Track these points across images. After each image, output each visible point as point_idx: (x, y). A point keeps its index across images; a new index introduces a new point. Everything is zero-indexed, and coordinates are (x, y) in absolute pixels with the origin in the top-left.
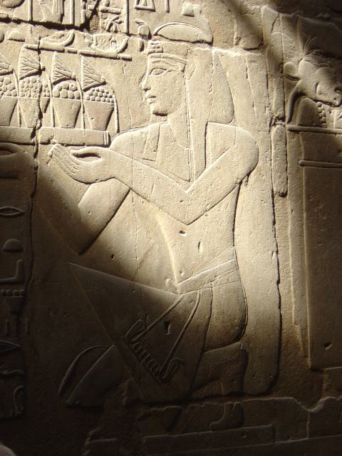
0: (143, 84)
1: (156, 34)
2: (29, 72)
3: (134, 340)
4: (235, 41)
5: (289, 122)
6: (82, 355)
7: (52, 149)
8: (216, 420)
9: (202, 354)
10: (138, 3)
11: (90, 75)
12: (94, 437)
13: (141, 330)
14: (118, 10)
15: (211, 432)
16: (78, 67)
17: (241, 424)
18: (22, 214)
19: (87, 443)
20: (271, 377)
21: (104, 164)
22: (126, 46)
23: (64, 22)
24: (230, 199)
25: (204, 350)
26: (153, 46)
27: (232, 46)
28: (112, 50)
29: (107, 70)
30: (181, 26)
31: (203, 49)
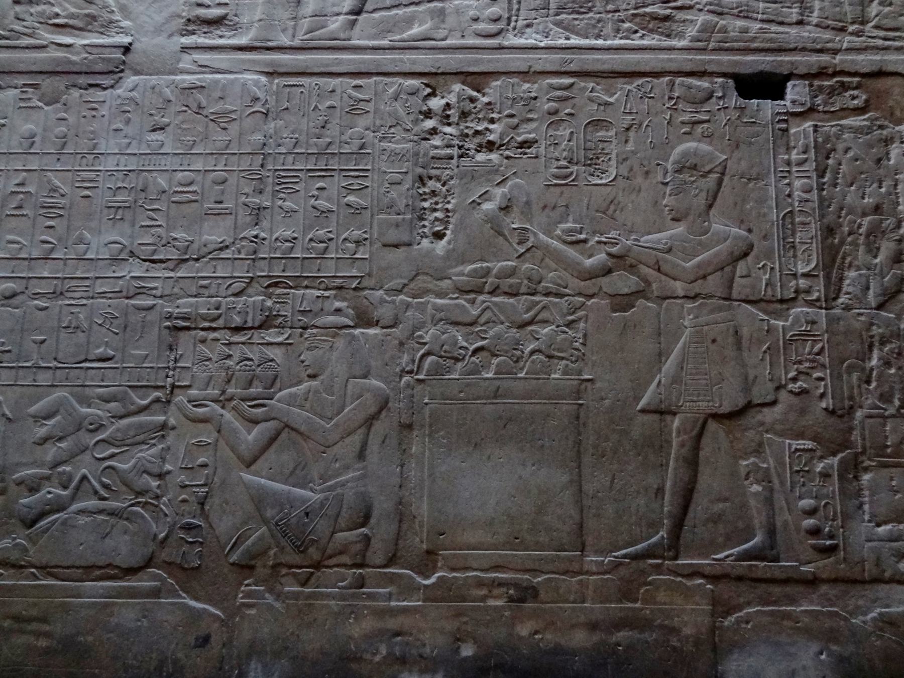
0: (302, 357)
5: (417, 374)
12: (247, 585)
16: (253, 353)
17: (362, 587)
19: (243, 588)
22: (290, 336)
25: (333, 533)
28: (280, 339)
29: (276, 354)
30: (331, 319)
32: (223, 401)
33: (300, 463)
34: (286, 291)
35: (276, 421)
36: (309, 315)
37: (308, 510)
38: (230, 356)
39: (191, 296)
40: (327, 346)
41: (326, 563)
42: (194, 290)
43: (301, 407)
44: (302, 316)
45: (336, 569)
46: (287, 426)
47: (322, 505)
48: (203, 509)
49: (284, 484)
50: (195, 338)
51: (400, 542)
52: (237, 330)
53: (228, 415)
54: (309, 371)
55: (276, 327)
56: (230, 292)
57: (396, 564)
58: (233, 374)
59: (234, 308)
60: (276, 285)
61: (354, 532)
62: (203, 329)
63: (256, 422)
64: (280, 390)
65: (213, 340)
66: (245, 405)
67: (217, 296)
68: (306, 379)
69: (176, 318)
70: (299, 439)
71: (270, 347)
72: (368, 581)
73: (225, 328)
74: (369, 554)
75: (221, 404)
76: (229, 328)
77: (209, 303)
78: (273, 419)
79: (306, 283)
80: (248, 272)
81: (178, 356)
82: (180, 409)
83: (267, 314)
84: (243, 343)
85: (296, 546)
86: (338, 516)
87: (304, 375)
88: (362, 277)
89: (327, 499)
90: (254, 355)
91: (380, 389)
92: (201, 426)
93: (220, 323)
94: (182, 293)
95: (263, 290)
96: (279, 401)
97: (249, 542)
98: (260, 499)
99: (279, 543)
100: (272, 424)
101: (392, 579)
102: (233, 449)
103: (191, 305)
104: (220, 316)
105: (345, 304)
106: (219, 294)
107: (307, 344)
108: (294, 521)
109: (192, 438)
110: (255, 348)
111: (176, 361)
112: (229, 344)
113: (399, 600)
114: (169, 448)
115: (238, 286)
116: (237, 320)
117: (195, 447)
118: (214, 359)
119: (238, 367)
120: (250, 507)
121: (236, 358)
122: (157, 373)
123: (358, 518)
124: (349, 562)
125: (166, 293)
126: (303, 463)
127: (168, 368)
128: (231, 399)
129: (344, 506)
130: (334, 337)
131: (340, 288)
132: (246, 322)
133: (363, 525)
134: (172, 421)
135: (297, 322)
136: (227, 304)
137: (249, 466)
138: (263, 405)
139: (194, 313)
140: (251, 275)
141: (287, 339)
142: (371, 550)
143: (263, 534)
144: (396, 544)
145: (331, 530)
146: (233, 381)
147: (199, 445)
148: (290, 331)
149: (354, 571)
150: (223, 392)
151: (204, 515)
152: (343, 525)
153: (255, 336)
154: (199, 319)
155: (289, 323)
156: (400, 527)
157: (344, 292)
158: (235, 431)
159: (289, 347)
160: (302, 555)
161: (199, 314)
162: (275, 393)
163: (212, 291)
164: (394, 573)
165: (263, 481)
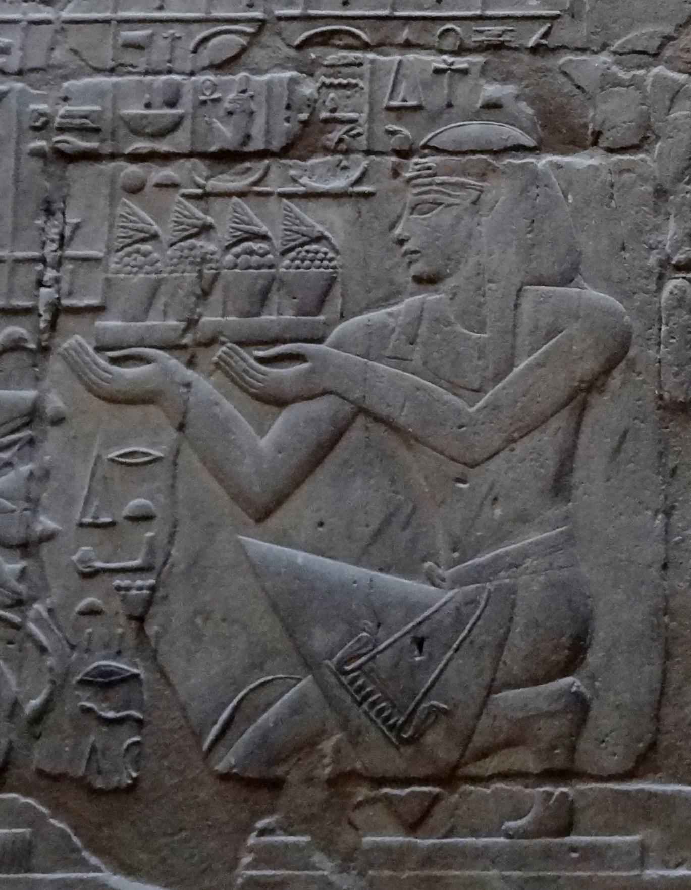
0: (397, 231)
1: (425, 147)
2: (186, 233)
3: (348, 668)
4: (590, 139)
6: (252, 690)
7: (219, 353)
8: (516, 819)
9: (488, 696)
10: (391, 98)
11: (295, 228)
13: (364, 650)
14: (353, 115)
15: (502, 839)
16: (270, 220)
17: (568, 829)
18: (157, 460)
20: (641, 745)
21: (312, 371)
23: (246, 149)
24: (561, 422)
25: (491, 689)
26: (418, 167)
27: (585, 148)
28: (339, 183)
30: (474, 128)
31: (518, 162)
32: (190, 347)
33: (398, 508)
34: (352, 55)
35: (331, 398)
36: (419, 117)
37: (424, 629)
38: (206, 229)
39: (98, 70)
40: (464, 198)
41: (472, 770)
42: (107, 57)
43: (399, 360)
44: (399, 120)
45: (499, 785)
46: (361, 410)
47: (459, 619)
48: (141, 630)
49: (357, 563)
50: (113, 181)
51: (665, 711)
52: (226, 158)
53: (205, 384)
54: (418, 268)
55: (327, 150)
56: (205, 57)
57: (656, 770)
58: (215, 277)
59: (216, 101)
60: (324, 39)
61: (541, 688)
62: (135, 158)
63: (281, 403)
64: (343, 317)
65: (159, 185)
66: (249, 357)
67: (170, 72)
68: (412, 286)
69: (61, 130)
70: (392, 442)
71: (312, 204)
72: (583, 819)
73: (190, 155)
74: (584, 745)
75: (186, 356)
76: (203, 156)
77: (150, 87)
78: (325, 393)
79: (405, 34)
80: (250, 6)
81: (67, 233)
82: (77, 370)
83: (304, 116)
84: (242, 194)
85: (391, 728)
86: (501, 647)
87: (404, 277)
88: (557, 17)
89: (472, 602)
90: (271, 224)
91: (608, 312)
92: (135, 413)
93: (180, 141)
94: (74, 63)
95: (292, 53)
96: (337, 346)
97: (267, 718)
98: (293, 605)
99: (347, 720)
100: (321, 407)
101: (646, 809)
102: (220, 473)
103: (99, 94)
104: (176, 125)
105: (510, 89)
106: (176, 66)
107: (411, 195)
108: (385, 661)
109: (108, 446)
110: (272, 204)
111: (62, 242)
112: (205, 197)
113: (666, 865)
114: (47, 474)
115: (226, 44)
116: (225, 135)
117: (117, 471)
118: (165, 237)
119: (229, 258)
120: (267, 627)
121: (223, 234)
122: (12, 273)
123: (556, 649)
124: (533, 765)
125: (31, 64)
126: (408, 510)
127: (43, 260)
128: (210, 343)
129: (520, 620)
130: (482, 176)
131: (497, 47)
132: (248, 137)
133: (569, 667)
134: (55, 403)
135: (385, 138)
136: (198, 90)
137: (263, 515)
138: (298, 358)
139: (109, 115)
140: (258, 14)
141: (359, 181)
142: (590, 733)
143: (303, 695)
144: (657, 718)
145: (486, 678)
146: (217, 295)
147: (130, 464)
148: (365, 163)
149: (548, 788)
150: (191, 323)
151: (145, 646)
152: (516, 670)
153: (272, 175)
154: (122, 131)
155: (363, 140)
156: (665, 673)
157: (507, 57)
158: (224, 427)
159: (364, 205)
160: (409, 750)
161: (121, 118)
162: (329, 325)
163: (157, 55)
164: (652, 795)
165: (301, 557)
